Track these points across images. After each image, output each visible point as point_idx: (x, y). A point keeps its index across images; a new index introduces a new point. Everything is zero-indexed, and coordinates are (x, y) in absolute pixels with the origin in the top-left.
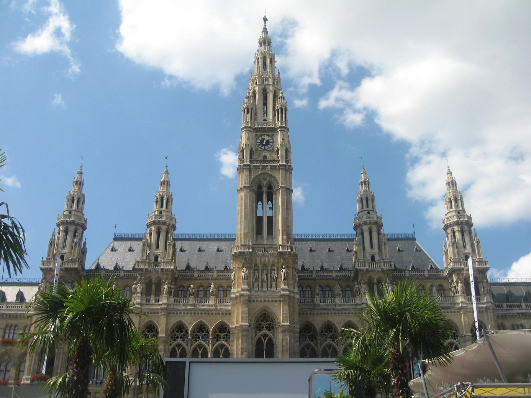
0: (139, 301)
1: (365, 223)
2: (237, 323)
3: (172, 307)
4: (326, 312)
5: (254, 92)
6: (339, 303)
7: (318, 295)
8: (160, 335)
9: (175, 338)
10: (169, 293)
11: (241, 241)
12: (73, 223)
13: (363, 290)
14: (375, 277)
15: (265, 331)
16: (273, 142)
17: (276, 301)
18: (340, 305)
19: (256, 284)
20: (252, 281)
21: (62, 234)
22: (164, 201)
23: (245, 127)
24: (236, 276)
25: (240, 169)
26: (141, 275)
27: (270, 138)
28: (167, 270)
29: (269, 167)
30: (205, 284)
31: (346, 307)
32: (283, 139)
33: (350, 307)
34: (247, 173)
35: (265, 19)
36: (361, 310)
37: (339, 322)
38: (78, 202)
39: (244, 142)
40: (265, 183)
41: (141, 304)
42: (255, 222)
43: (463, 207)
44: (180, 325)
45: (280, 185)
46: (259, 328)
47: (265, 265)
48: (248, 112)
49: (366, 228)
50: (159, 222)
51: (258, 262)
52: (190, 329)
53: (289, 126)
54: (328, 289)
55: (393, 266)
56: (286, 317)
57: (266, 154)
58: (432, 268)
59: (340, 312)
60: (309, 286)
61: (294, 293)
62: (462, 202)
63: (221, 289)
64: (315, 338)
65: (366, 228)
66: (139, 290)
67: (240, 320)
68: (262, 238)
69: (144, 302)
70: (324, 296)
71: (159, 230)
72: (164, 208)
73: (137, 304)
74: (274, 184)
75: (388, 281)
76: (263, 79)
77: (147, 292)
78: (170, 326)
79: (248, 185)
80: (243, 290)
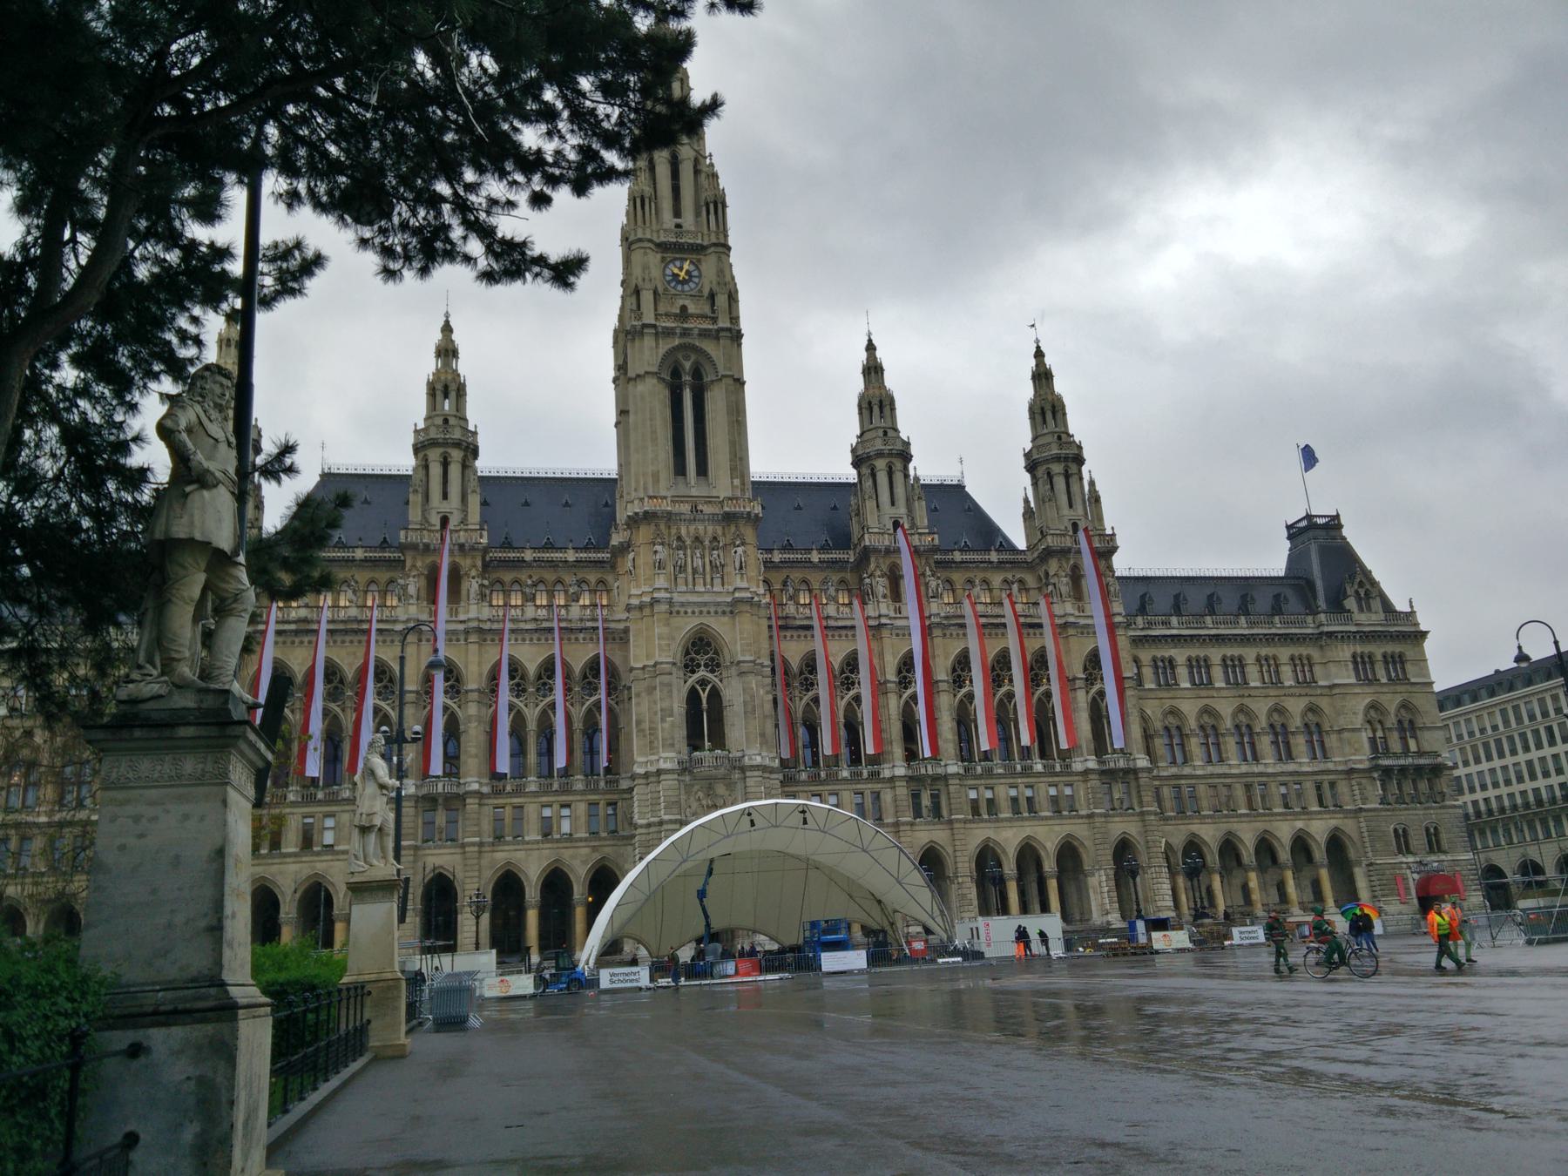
1: (880, 454)
2: (648, 657)
3: (487, 626)
11: (645, 489)
16: (700, 276)
17: (724, 613)
24: (640, 561)
26: (414, 558)
27: (692, 268)
28: (473, 549)
29: (696, 332)
34: (649, 341)
40: (687, 365)
42: (669, 447)
43: (1066, 425)
45: (722, 372)
46: (690, 667)
47: (697, 539)
49: (881, 464)
50: (445, 444)
51: (683, 532)
53: (731, 243)
54: (804, 587)
55: (937, 542)
56: (749, 645)
57: (687, 302)
62: (1064, 414)
65: (881, 464)
66: (412, 590)
71: (445, 459)
75: (928, 573)
79: (655, 369)
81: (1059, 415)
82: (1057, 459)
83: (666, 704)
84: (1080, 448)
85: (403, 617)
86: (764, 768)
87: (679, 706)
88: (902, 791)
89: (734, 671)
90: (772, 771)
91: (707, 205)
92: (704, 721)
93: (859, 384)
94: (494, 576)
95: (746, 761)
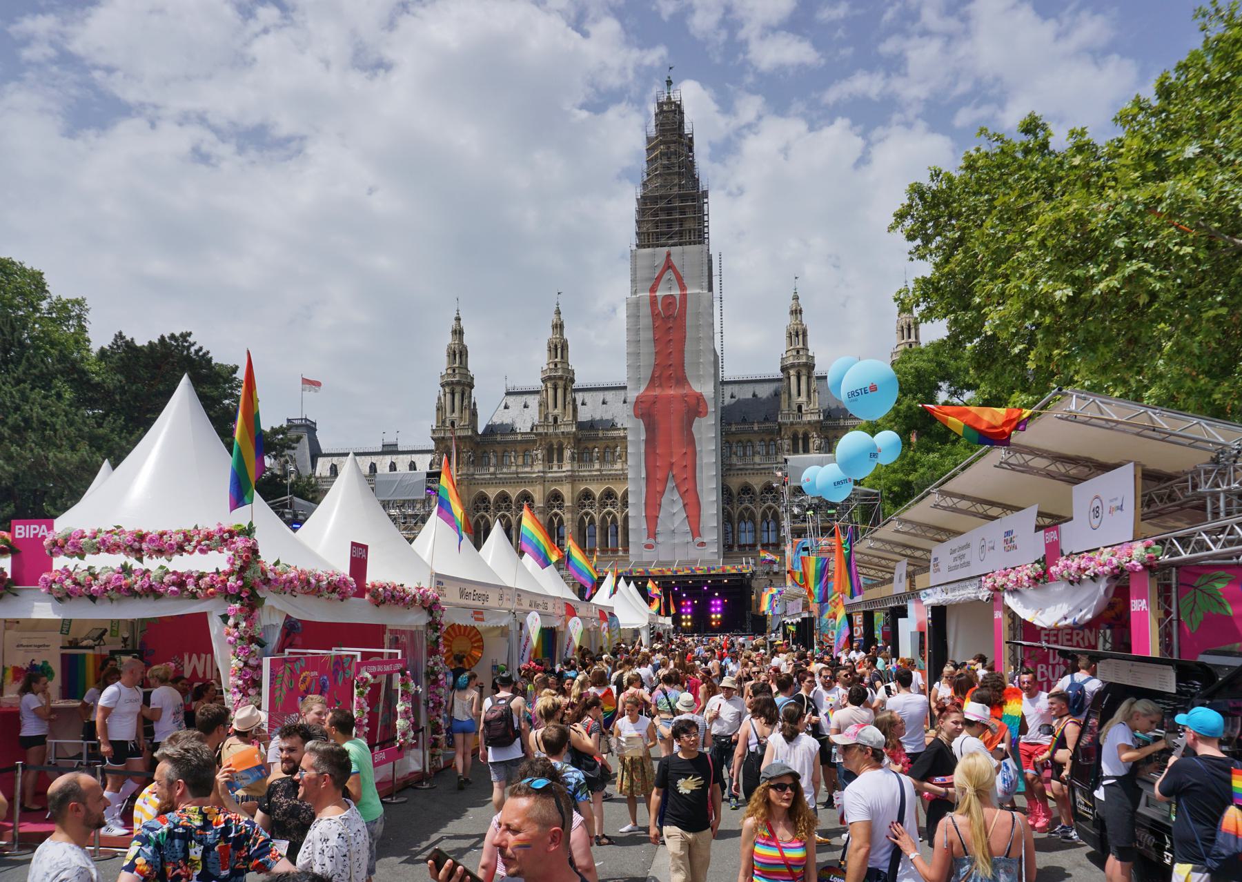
1: (793, 366)
8: (566, 504)
10: (573, 459)
12: (458, 383)
13: (786, 447)
21: (448, 396)
28: (568, 433)
30: (611, 444)
37: (757, 483)
43: (917, 337)
49: (792, 372)
52: (597, 495)
70: (745, 454)
72: (559, 359)
77: (548, 459)
78: (576, 494)
93: (787, 321)
94: (583, 446)
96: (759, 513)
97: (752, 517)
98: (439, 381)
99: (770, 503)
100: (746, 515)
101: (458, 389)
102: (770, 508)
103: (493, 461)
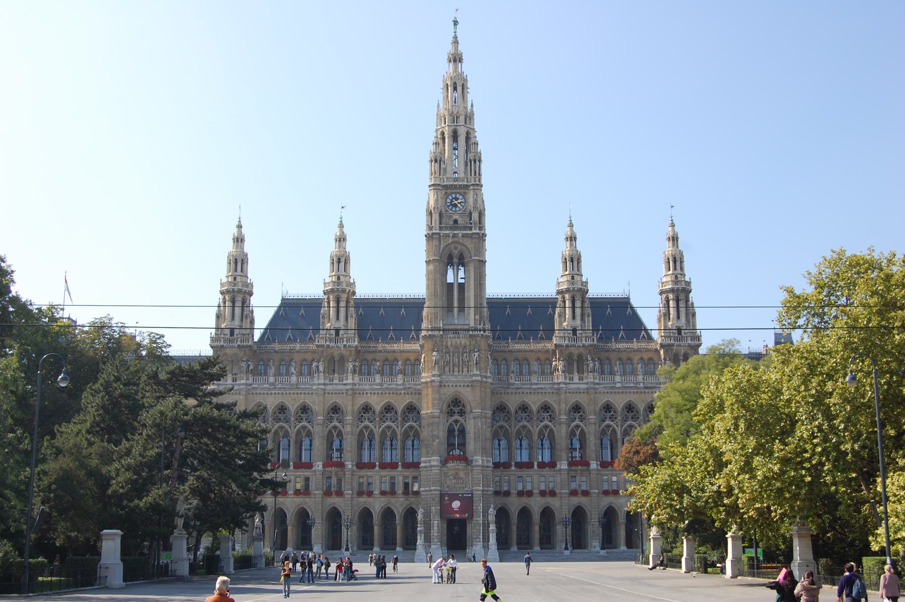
0: (322, 381)
1: (568, 291)
4: (520, 391)
5: (443, 133)
6: (536, 382)
7: (513, 372)
9: (360, 419)
10: (354, 372)
12: (240, 291)
14: (575, 352)
15: (456, 417)
16: (465, 202)
18: (537, 384)
19: (447, 369)
20: (443, 366)
22: (341, 261)
23: (433, 185)
25: (429, 237)
27: (461, 197)
28: (350, 346)
30: (391, 357)
31: (543, 386)
32: (476, 201)
33: (547, 386)
34: (436, 242)
35: (456, 23)
36: (559, 389)
37: (534, 403)
38: (242, 264)
39: (432, 203)
40: (456, 252)
41: (324, 384)
43: (682, 269)
44: (367, 406)
46: (451, 413)
48: (436, 161)
49: (567, 296)
51: (449, 343)
53: (483, 182)
54: (526, 362)
55: (595, 342)
58: (644, 337)
59: (535, 392)
60: (505, 359)
61: (486, 377)
62: (681, 262)
63: (408, 362)
64: (509, 419)
66: (321, 368)
67: (430, 405)
68: (453, 316)
69: (327, 382)
70: (521, 373)
73: (319, 384)
74: (466, 254)
76: (455, 118)
80: (434, 376)
81: (678, 264)
82: (672, 291)
83: (435, 433)
84: (688, 283)
85: (316, 381)
86: (483, 466)
87: (442, 434)
88: (565, 476)
89: (472, 416)
90: (488, 467)
91: (471, 161)
92: (456, 440)
95: (474, 464)
96: (535, 431)
97: (529, 435)
98: (218, 288)
99: (546, 422)
100: (524, 433)
101: (239, 299)
102: (546, 427)
103: (272, 371)
